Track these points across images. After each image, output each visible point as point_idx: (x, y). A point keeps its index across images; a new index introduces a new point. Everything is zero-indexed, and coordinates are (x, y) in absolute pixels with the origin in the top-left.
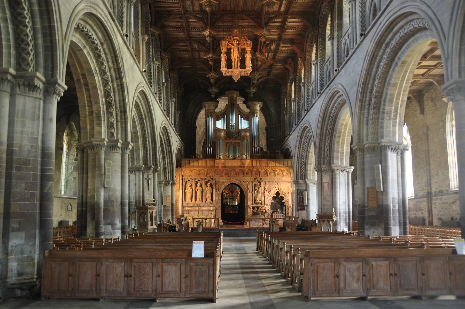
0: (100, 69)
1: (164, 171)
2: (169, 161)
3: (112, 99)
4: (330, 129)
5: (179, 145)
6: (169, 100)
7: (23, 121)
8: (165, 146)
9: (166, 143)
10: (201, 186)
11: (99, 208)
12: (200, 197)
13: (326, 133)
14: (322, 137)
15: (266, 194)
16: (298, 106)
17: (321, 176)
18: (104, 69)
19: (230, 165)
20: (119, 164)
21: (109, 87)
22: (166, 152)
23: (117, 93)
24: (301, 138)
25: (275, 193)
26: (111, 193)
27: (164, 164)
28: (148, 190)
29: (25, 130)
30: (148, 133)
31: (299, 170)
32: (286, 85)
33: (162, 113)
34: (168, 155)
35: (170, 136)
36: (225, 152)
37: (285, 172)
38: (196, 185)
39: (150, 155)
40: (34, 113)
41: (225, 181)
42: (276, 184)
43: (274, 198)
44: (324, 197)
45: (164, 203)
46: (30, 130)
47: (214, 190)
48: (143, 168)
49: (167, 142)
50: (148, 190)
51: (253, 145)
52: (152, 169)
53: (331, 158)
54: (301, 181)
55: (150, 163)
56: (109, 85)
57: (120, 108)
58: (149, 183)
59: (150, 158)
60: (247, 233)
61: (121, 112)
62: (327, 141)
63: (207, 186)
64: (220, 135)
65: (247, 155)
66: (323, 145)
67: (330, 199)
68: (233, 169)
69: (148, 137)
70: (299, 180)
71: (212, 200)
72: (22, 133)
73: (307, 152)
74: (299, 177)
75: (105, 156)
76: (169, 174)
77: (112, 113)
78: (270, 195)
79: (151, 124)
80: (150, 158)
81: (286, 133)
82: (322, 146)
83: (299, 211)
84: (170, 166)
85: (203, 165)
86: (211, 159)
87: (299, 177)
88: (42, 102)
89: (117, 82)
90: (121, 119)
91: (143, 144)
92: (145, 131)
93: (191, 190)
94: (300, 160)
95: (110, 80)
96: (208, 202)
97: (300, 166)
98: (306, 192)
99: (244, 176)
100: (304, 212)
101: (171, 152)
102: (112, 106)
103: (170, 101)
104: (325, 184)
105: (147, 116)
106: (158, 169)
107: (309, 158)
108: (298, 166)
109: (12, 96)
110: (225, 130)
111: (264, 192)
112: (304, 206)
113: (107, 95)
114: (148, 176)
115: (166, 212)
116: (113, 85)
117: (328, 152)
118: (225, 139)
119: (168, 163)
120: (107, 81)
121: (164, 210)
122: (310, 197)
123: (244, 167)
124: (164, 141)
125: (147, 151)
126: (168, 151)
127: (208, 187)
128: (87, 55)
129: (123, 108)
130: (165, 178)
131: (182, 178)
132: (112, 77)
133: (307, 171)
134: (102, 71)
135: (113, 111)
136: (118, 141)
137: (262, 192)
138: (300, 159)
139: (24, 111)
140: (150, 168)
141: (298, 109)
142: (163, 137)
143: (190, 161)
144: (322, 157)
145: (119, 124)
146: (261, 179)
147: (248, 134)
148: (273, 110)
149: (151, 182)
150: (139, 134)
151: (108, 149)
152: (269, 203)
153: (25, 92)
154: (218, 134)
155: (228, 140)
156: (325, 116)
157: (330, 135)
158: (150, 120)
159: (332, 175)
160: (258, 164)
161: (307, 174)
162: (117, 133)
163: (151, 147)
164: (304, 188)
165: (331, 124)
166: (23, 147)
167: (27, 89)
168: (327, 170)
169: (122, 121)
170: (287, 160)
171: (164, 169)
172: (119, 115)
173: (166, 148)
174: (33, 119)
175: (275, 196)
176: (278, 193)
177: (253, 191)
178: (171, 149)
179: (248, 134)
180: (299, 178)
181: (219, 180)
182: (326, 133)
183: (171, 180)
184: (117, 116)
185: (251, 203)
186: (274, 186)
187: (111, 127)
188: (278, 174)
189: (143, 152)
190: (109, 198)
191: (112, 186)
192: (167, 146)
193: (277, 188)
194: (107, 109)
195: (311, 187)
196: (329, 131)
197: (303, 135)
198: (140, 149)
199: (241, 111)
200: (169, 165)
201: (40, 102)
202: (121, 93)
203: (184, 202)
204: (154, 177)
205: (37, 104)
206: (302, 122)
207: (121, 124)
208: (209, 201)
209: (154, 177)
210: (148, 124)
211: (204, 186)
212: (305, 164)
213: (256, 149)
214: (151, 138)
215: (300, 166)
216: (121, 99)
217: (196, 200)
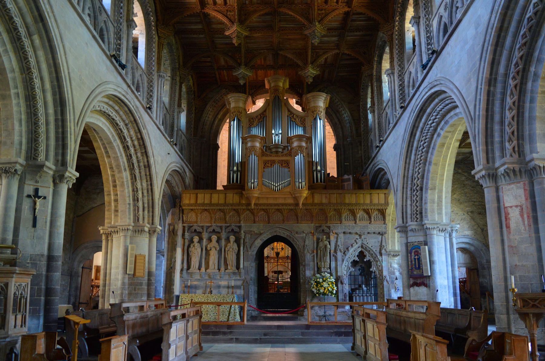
1: (135, 205)
2: (145, 185)
4: (521, 58)
8: (136, 154)
9: (138, 147)
10: (218, 241)
12: (216, 262)
13: (506, 75)
14: (495, 86)
15: (339, 255)
16: (400, 80)
17: (497, 189)
19: (271, 201)
22: (139, 166)
24: (412, 135)
25: (357, 254)
27: (133, 190)
28: (34, 225)
30: (42, 79)
31: (409, 202)
32: (370, 62)
33: (108, 63)
34: (143, 173)
35: (144, 132)
36: (263, 177)
37: (375, 214)
38: (210, 240)
39: (48, 138)
41: (262, 231)
42: (358, 237)
43: (354, 263)
44: (511, 247)
45: (130, 271)
47: (242, 248)
49: (140, 145)
50: (34, 225)
51: (314, 168)
52: (51, 173)
53: (523, 139)
54: (412, 224)
58: (38, 207)
59: (47, 146)
60: (303, 334)
62: (512, 93)
63: (229, 242)
64: (253, 147)
65: (304, 183)
66: (497, 109)
67: (533, 250)
68: (278, 210)
69: (44, 91)
70: (410, 223)
71: (238, 267)
73: (425, 164)
74: (409, 216)
76: (146, 212)
78: (347, 257)
79: (50, 56)
80: (47, 146)
81: (374, 145)
82: (493, 111)
83: (412, 289)
84: (148, 196)
85: (222, 201)
86: (236, 191)
87: (409, 216)
91: (27, 105)
93: (199, 250)
94: (409, 182)
96: (231, 271)
97: (409, 195)
98: (427, 247)
99: (297, 223)
100: (422, 290)
101: (148, 166)
103: (155, 73)
104: (510, 210)
105: (33, 29)
106: (67, 174)
107: (430, 175)
108: (406, 194)
110: (262, 138)
111: (335, 251)
112: (422, 276)
114: (36, 190)
115: (135, 290)
117: (515, 124)
118: (263, 154)
122: (436, 258)
123: (297, 205)
124: (132, 141)
126: (142, 164)
127: (232, 242)
130: (136, 219)
133: (426, 203)
137: (332, 252)
138: (410, 179)
141: (400, 85)
142: (129, 131)
143: (197, 194)
144: (497, 139)
146: (329, 227)
147: (304, 144)
148: (346, 116)
149: (44, 206)
150: (10, 75)
152: (345, 273)
154: (249, 144)
155: (267, 155)
156: (505, 25)
157: (519, 78)
158: (47, 44)
159: (532, 184)
160: (324, 201)
161: (426, 209)
163: (52, 119)
164: (421, 239)
165: (525, 44)
168: (514, 171)
170: (378, 191)
171: (134, 200)
173: (137, 158)
175: (357, 259)
176: (361, 255)
177: (315, 252)
178: (148, 161)
179: (304, 144)
180: (409, 220)
181: (252, 229)
182: (506, 75)
185: (312, 272)
186: (354, 242)
188: (361, 219)
189: (28, 127)
193: (360, 244)
195: (435, 236)
196: (517, 64)
197: (418, 127)
198: (16, 116)
199: (292, 110)
200: (145, 194)
203: (185, 271)
204: (55, 193)
206: (418, 93)
208: (232, 268)
209: (55, 193)
210: (41, 53)
211: (223, 243)
212: (421, 189)
213: (319, 175)
214: (54, 94)
215: (409, 195)
217: (207, 268)
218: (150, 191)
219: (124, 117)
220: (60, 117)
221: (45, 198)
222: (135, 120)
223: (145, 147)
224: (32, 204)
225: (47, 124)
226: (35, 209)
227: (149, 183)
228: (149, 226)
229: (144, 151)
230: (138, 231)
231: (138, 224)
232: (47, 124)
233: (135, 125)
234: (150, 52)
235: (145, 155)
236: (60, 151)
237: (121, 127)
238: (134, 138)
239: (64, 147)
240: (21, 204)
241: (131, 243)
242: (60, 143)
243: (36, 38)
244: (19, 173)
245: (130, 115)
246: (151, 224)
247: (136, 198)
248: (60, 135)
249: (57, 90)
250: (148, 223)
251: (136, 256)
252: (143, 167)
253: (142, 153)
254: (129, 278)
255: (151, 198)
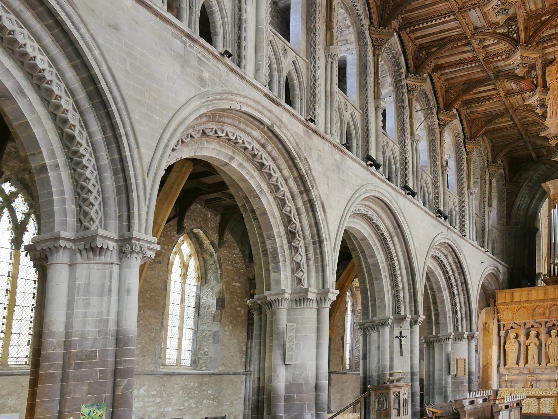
0: (269, 183)
1: (454, 317)
2: (462, 298)
3: (296, 227)
5: (492, 268)
6: (463, 194)
7: (87, 299)
8: (454, 275)
11: (278, 397)
18: (275, 183)
20: (314, 325)
21: (289, 209)
22: (457, 284)
23: (304, 216)
26: (297, 372)
27: (452, 305)
28: (401, 355)
29: (89, 311)
30: (399, 261)
33: (434, 221)
34: (460, 289)
35: (461, 256)
39: (404, 298)
40: (103, 285)
46: (96, 310)
48: (390, 321)
49: (457, 267)
50: (401, 355)
52: (409, 320)
55: (406, 310)
56: (288, 206)
57: (312, 239)
59: (404, 302)
61: (314, 243)
69: (400, 269)
72: (85, 316)
75: (288, 314)
77: (296, 249)
80: (404, 302)
88: (115, 268)
89: (303, 198)
90: (315, 254)
92: (392, 259)
95: (290, 197)
101: (465, 283)
102: (295, 237)
109: (72, 265)
113: (287, 220)
114: (401, 333)
116: (296, 205)
119: (460, 302)
120: (284, 200)
121: (453, 383)
124: (451, 266)
125: (397, 291)
126: (459, 282)
128: (239, 170)
129: (316, 237)
130: (456, 328)
131: (499, 326)
132: (291, 193)
134: (272, 186)
135: (298, 244)
136: (306, 291)
139: (87, 285)
140: (403, 318)
142: (447, 259)
145: (312, 262)
149: (406, 341)
151: (292, 304)
153: (89, 259)
158: (402, 240)
162: (309, 277)
166: (87, 335)
167: (91, 253)
169: (317, 258)
171: (453, 313)
172: (311, 247)
173: (455, 278)
174: (101, 294)
178: (465, 279)
183: (467, 331)
184: (306, 251)
187: (297, 270)
190: (294, 379)
191: (299, 361)
192: (457, 275)
194: (289, 242)
200: (463, 306)
201: (112, 268)
202: (311, 214)
204: (412, 332)
205: (107, 271)
207: (316, 262)
209: (412, 332)
210: (398, 247)
214: (406, 268)
216: (313, 222)
218: (467, 303)
219: (444, 251)
220: (411, 282)
221: (406, 337)
222: (453, 250)
223: (462, 268)
224: (399, 342)
225: (403, 288)
226: (401, 345)
227: (466, 296)
228: (467, 333)
229: (461, 271)
230: (459, 338)
231: (458, 333)
232: (403, 288)
233: (453, 254)
234: (460, 173)
235: (462, 275)
236: (413, 305)
237: (442, 259)
238: (452, 263)
239: (416, 301)
240: (393, 343)
241: (452, 349)
242: (413, 299)
243: (396, 239)
244: (390, 324)
245: (449, 248)
246: (469, 331)
247: (455, 311)
248: (412, 294)
249: (409, 265)
250: (467, 331)
251: (457, 360)
252: (460, 284)
253: (459, 273)
254: (452, 378)
255: (468, 309)
